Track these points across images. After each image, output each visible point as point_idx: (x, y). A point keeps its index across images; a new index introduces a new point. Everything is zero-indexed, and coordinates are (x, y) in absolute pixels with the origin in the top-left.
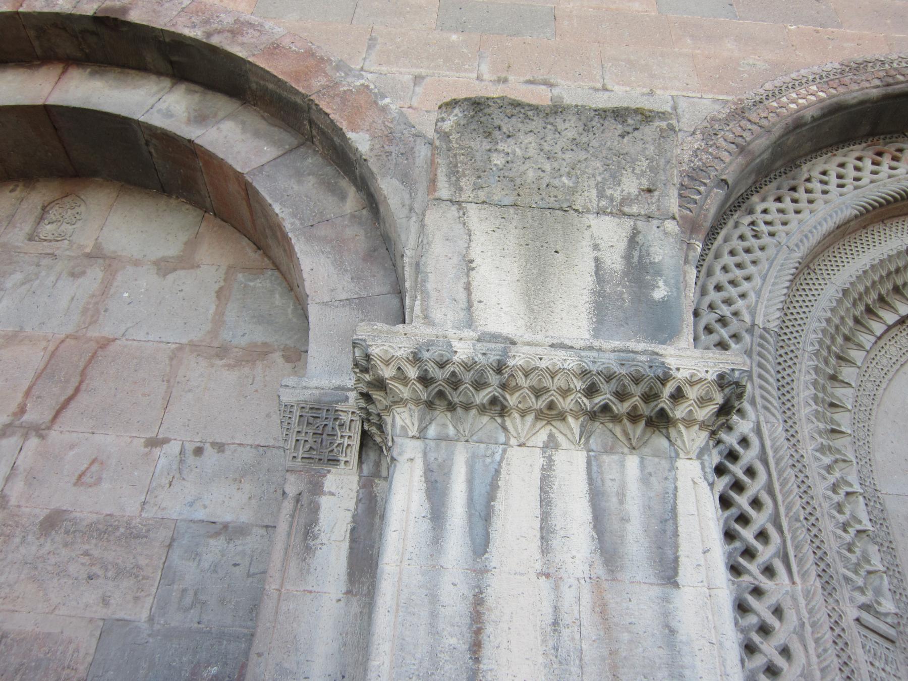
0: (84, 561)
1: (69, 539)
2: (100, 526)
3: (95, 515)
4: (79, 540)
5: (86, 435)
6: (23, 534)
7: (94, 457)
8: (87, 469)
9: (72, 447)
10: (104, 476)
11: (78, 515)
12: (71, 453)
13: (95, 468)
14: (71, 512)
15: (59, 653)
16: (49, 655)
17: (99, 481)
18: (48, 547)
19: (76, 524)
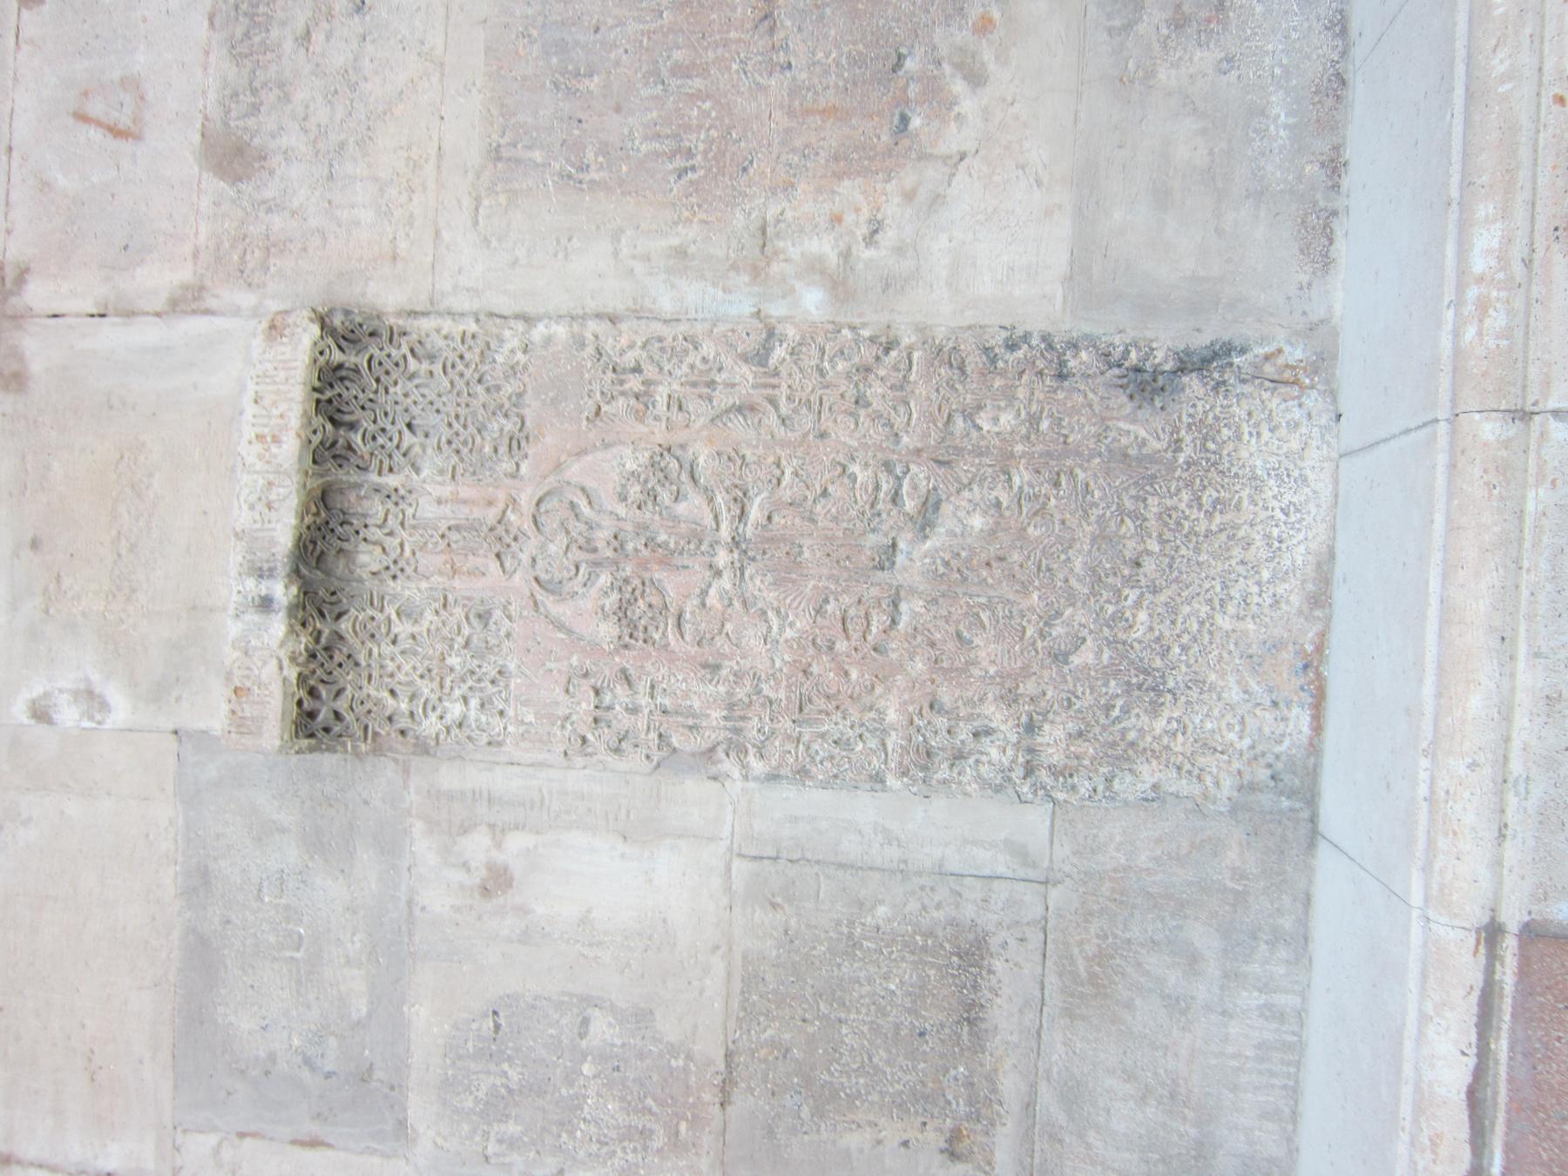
0: (322, 37)
1: (270, 97)
2: (239, 31)
3: (212, 58)
4: (273, 68)
5: (15, 164)
6: (262, 214)
7: (71, 121)
8: (99, 124)
9: (45, 185)
10: (116, 75)
11: (212, 96)
12: (62, 181)
13: (96, 108)
14: (206, 118)
15: (530, 12)
16: (535, 33)
17: (132, 84)
18: (292, 139)
19: (235, 95)
